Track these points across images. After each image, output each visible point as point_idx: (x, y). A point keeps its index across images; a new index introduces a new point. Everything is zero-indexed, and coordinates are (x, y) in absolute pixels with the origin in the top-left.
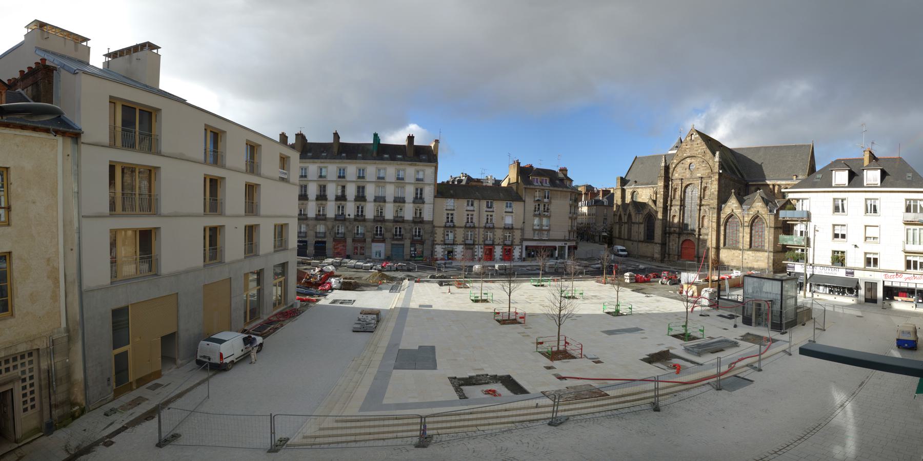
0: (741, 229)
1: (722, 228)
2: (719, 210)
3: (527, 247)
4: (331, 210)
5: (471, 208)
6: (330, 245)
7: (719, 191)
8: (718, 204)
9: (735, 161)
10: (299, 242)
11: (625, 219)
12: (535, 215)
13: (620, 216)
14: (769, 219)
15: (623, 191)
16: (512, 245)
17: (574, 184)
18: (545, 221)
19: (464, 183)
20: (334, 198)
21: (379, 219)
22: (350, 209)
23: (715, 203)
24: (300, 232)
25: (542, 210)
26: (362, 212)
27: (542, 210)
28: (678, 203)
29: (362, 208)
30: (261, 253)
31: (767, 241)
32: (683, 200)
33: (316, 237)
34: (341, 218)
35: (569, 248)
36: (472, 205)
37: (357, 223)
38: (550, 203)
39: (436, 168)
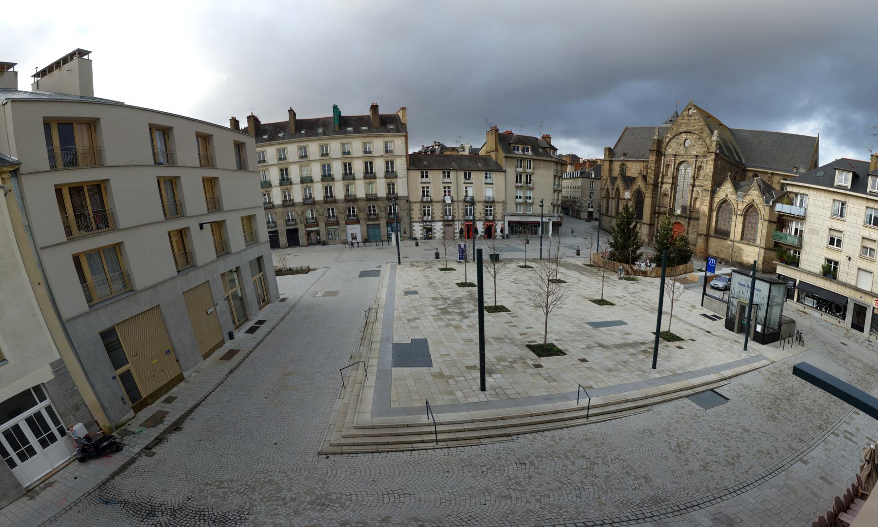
0: (734, 217)
1: (715, 214)
2: (713, 193)
3: (510, 223)
4: (297, 195)
5: (448, 180)
6: (302, 234)
7: (714, 173)
8: (712, 187)
9: (734, 143)
10: (269, 232)
11: (612, 194)
12: (517, 187)
13: (608, 189)
14: (764, 211)
15: (611, 162)
16: (493, 221)
17: (558, 153)
18: (529, 194)
19: (438, 152)
20: (299, 180)
21: (350, 199)
22: (318, 193)
23: (708, 184)
24: (269, 222)
25: (525, 181)
26: (331, 192)
27: (525, 181)
28: (670, 181)
29: (331, 188)
30: (233, 250)
31: (759, 234)
32: (675, 178)
33: (287, 225)
34: (309, 201)
35: (554, 223)
36: (448, 176)
37: (327, 206)
38: (533, 173)
39: (406, 137)
